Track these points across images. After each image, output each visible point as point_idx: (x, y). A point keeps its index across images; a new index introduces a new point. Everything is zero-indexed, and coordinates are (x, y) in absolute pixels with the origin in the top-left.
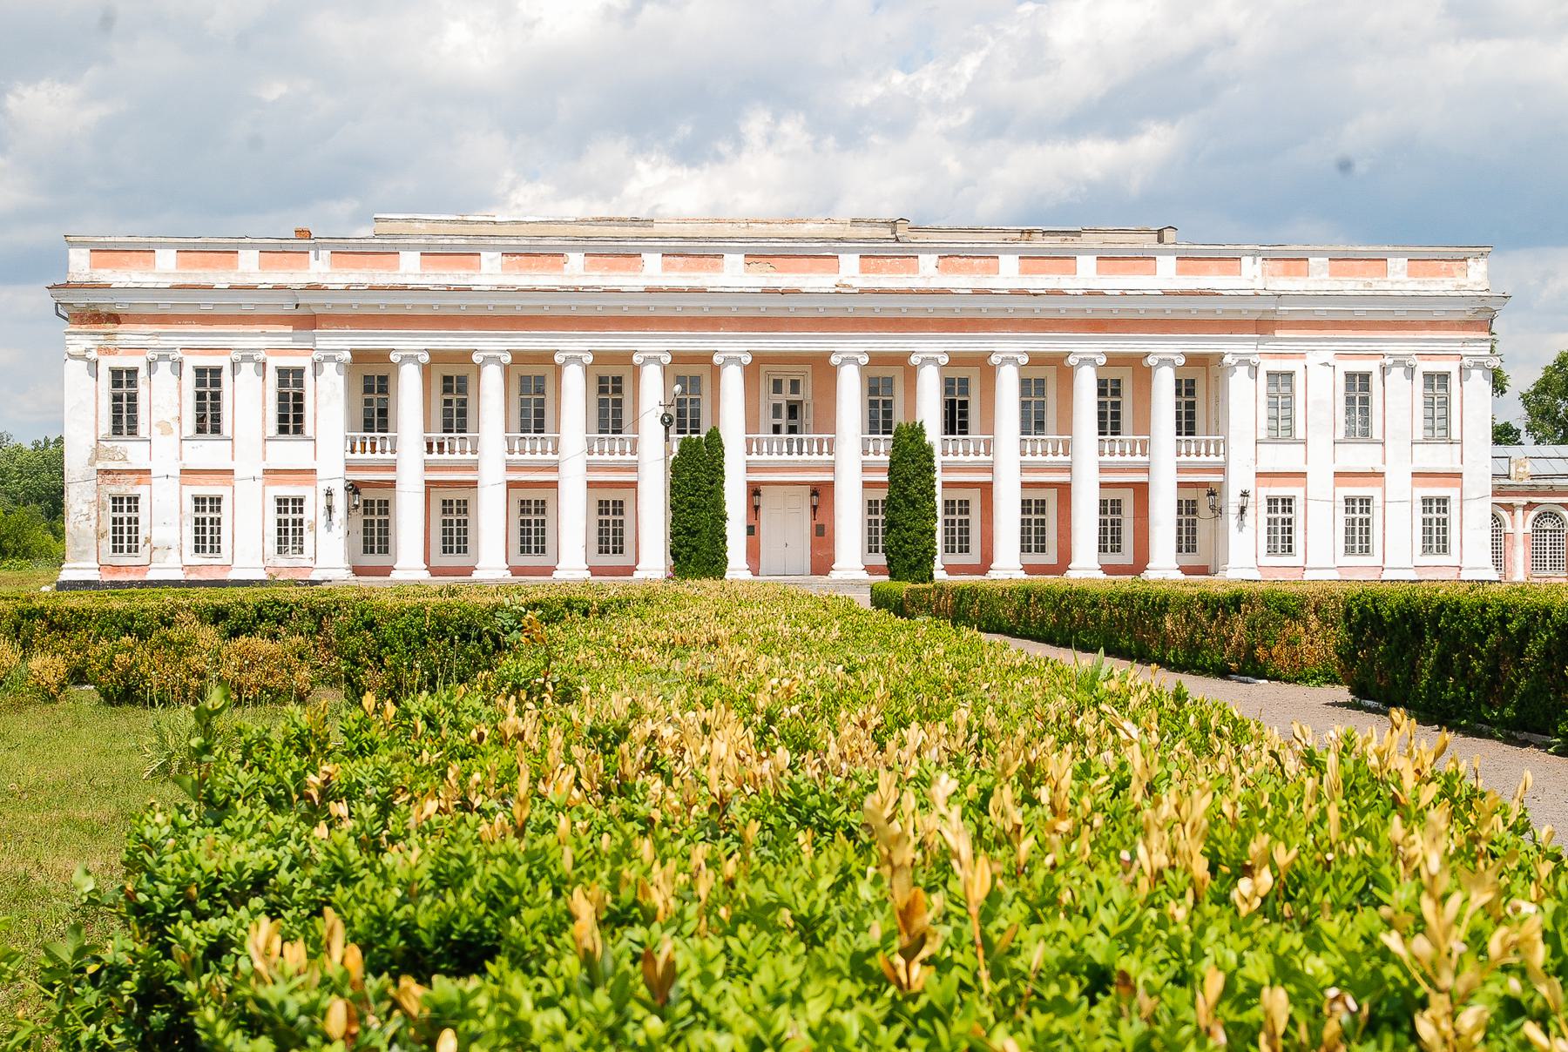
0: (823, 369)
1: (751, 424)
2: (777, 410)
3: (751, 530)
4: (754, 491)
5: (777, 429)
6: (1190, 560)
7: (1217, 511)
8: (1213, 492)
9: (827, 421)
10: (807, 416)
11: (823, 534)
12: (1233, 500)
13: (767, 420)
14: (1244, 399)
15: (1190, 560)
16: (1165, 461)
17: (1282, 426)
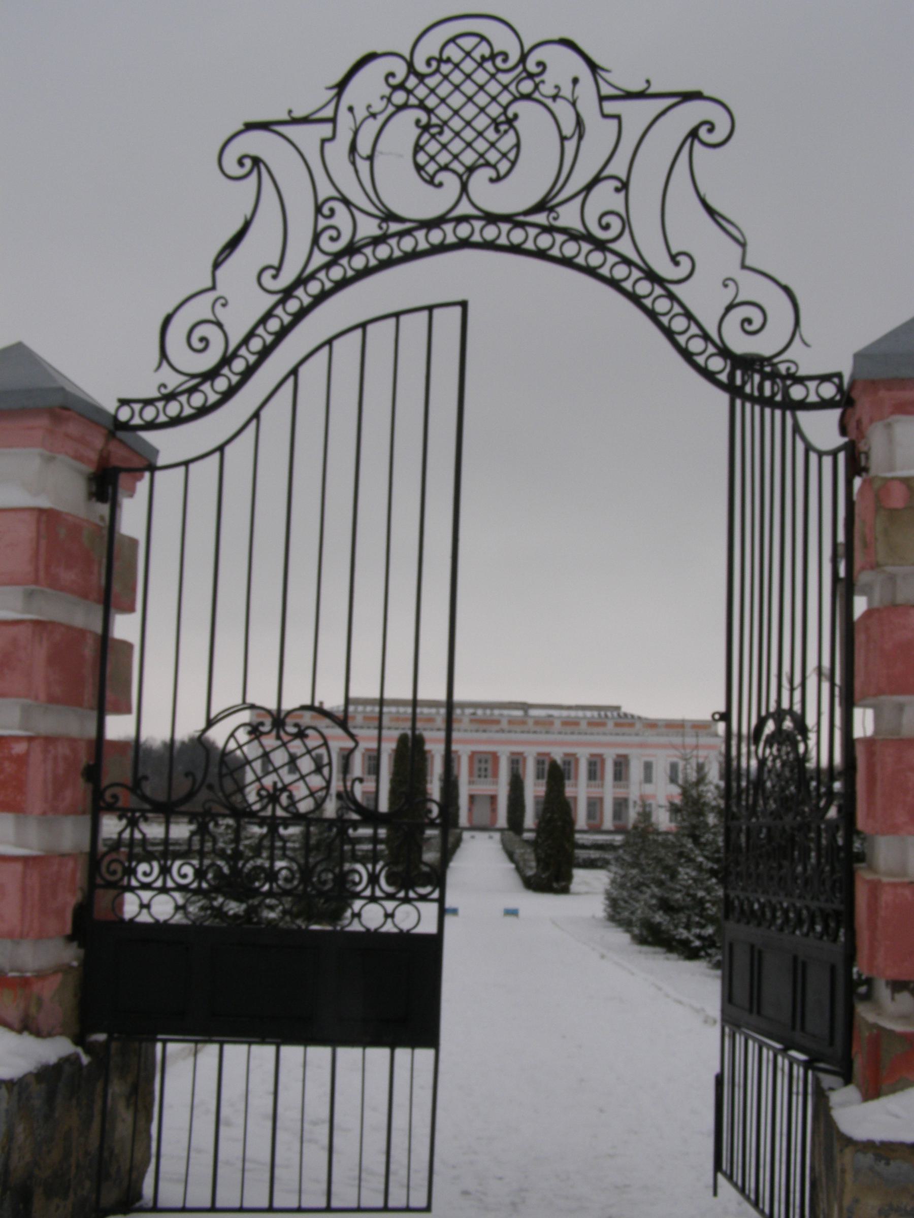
0: (495, 757)
1: (471, 773)
2: (480, 769)
3: (470, 810)
4: (472, 798)
5: (480, 776)
6: (618, 823)
7: (627, 806)
8: (626, 800)
9: (495, 774)
10: (489, 773)
11: (494, 810)
12: (631, 804)
13: (476, 772)
14: (636, 771)
15: (618, 823)
16: (609, 792)
17: (648, 778)
